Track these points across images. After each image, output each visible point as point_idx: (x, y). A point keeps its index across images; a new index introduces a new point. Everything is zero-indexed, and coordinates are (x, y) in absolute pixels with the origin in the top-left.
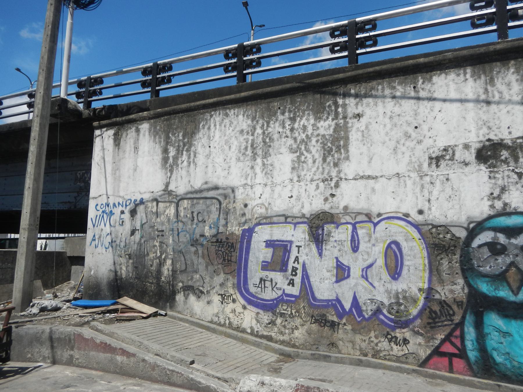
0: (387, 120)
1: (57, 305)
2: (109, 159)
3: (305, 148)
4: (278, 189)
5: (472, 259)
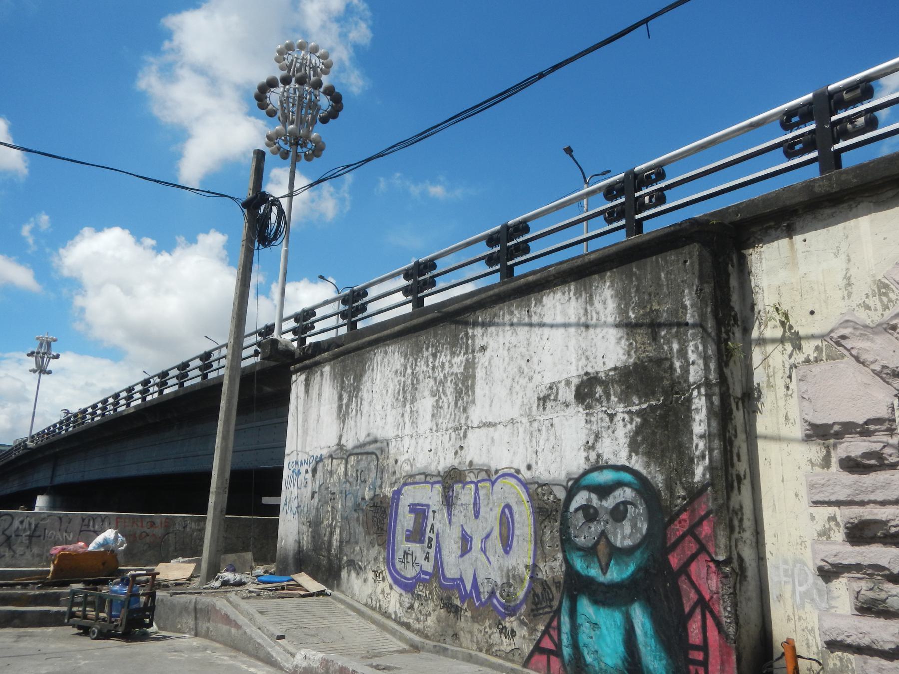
0: (506, 353)
1: (241, 579)
2: (300, 409)
3: (442, 389)
4: (421, 440)
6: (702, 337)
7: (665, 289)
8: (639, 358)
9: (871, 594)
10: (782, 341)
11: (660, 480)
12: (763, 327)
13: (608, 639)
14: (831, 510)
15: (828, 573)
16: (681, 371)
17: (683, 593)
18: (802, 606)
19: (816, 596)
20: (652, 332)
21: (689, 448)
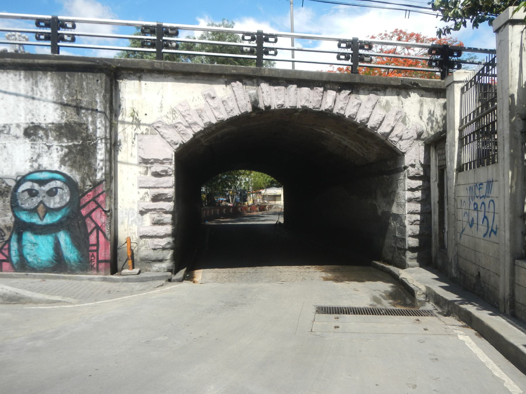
5: (17, 200)
6: (105, 118)
7: (85, 91)
9: (158, 218)
10: (132, 124)
12: (124, 116)
13: (43, 249)
14: (146, 190)
15: (142, 213)
17: (87, 225)
18: (132, 225)
19: (137, 221)
20: (76, 110)
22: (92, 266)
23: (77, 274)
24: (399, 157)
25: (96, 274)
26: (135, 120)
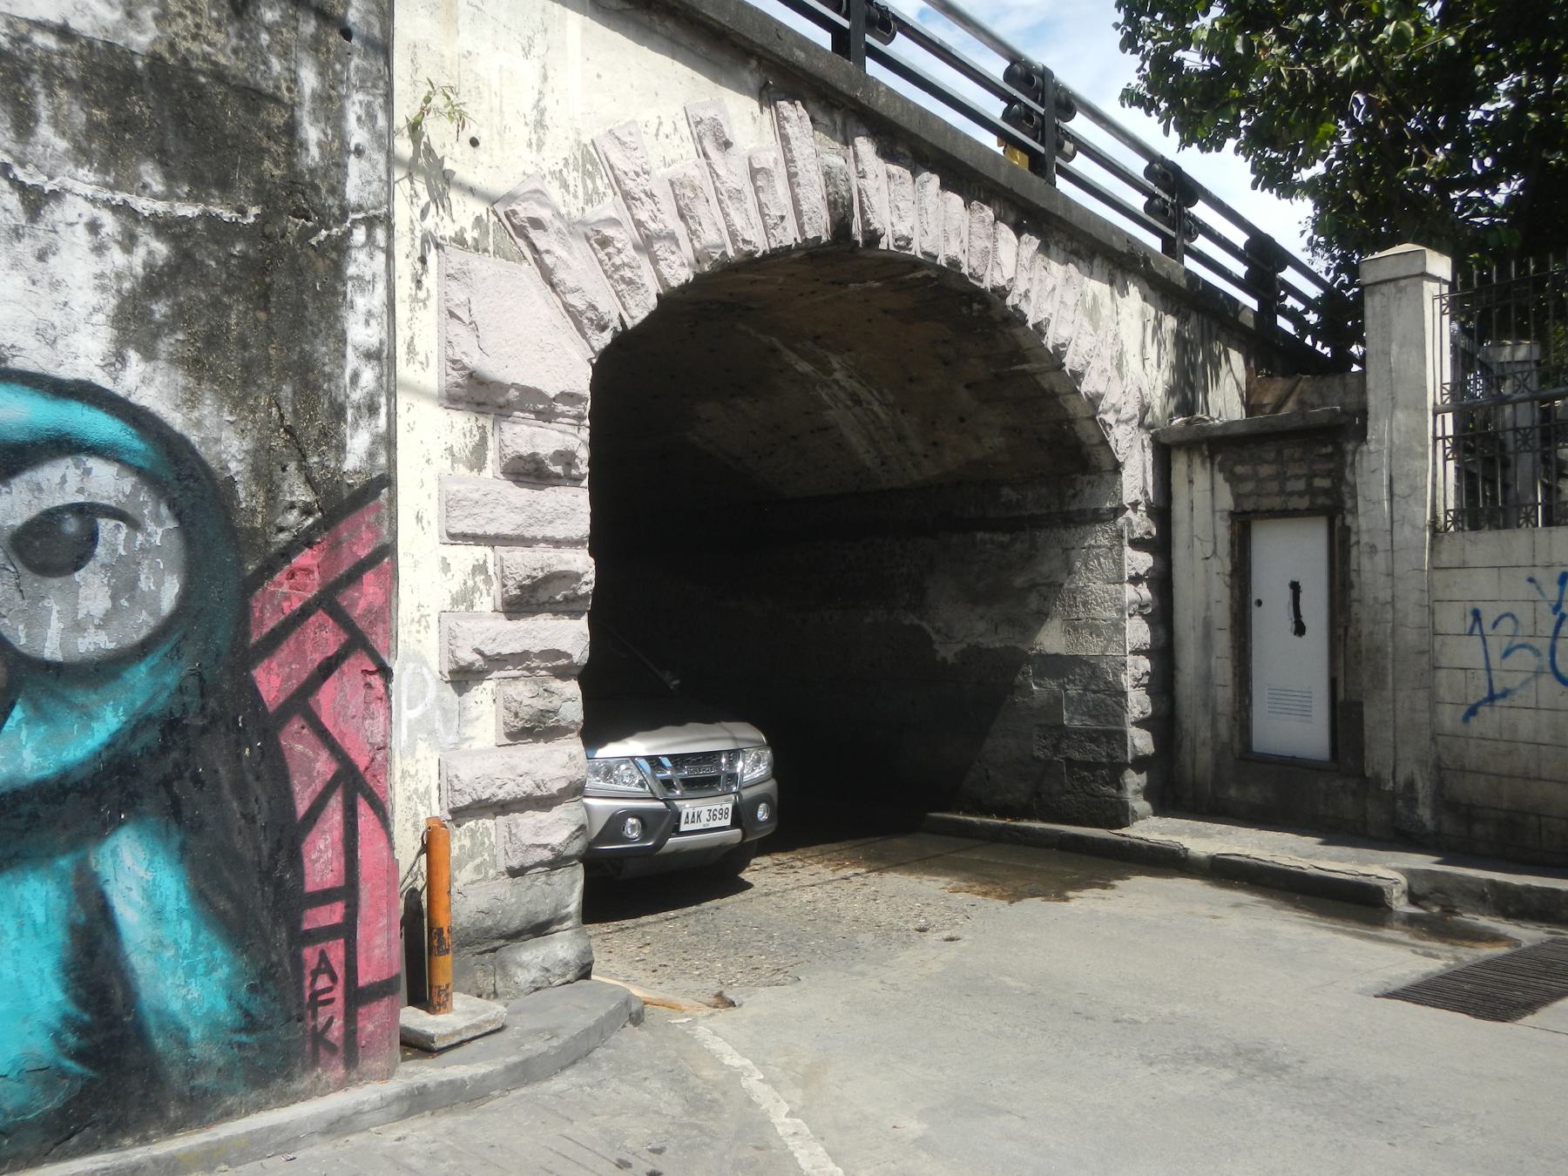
8: (172, 47)
9: (540, 704)
11: (233, 450)
16: (323, 157)
17: (293, 765)
21: (329, 377)
22: (318, 1037)
23: (228, 1115)
24: (1086, 478)
25: (342, 1085)
26: (422, 161)
